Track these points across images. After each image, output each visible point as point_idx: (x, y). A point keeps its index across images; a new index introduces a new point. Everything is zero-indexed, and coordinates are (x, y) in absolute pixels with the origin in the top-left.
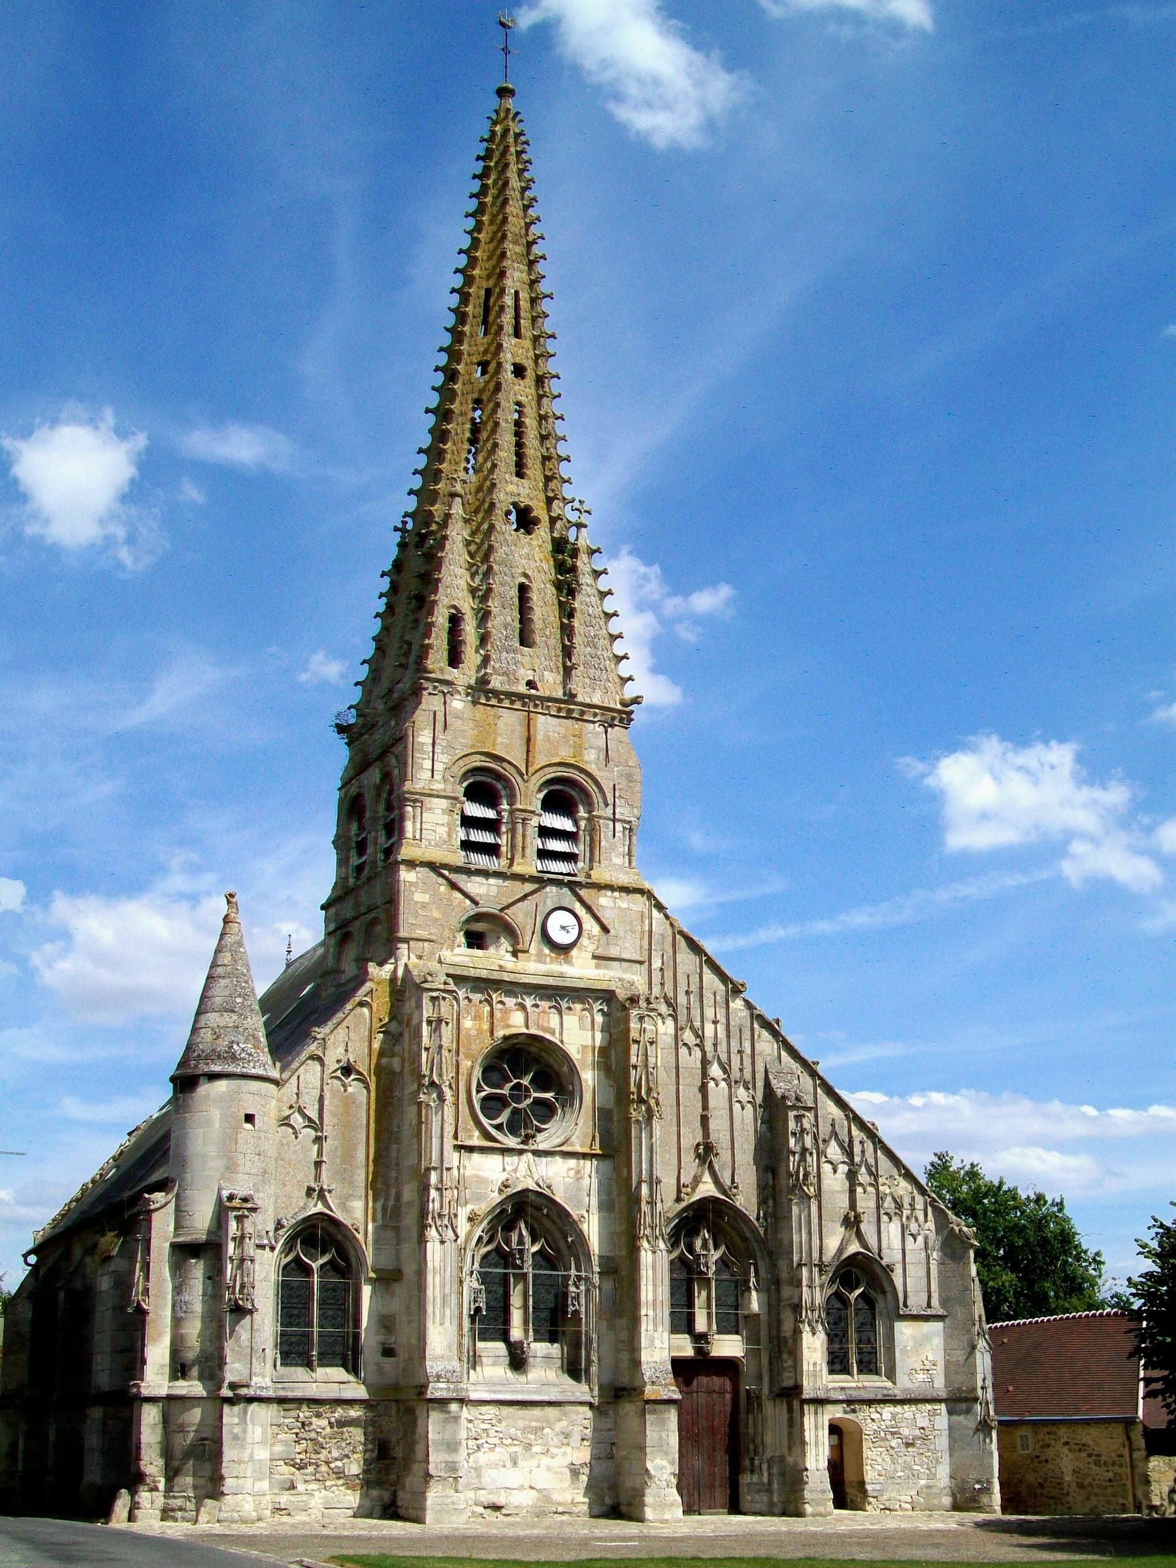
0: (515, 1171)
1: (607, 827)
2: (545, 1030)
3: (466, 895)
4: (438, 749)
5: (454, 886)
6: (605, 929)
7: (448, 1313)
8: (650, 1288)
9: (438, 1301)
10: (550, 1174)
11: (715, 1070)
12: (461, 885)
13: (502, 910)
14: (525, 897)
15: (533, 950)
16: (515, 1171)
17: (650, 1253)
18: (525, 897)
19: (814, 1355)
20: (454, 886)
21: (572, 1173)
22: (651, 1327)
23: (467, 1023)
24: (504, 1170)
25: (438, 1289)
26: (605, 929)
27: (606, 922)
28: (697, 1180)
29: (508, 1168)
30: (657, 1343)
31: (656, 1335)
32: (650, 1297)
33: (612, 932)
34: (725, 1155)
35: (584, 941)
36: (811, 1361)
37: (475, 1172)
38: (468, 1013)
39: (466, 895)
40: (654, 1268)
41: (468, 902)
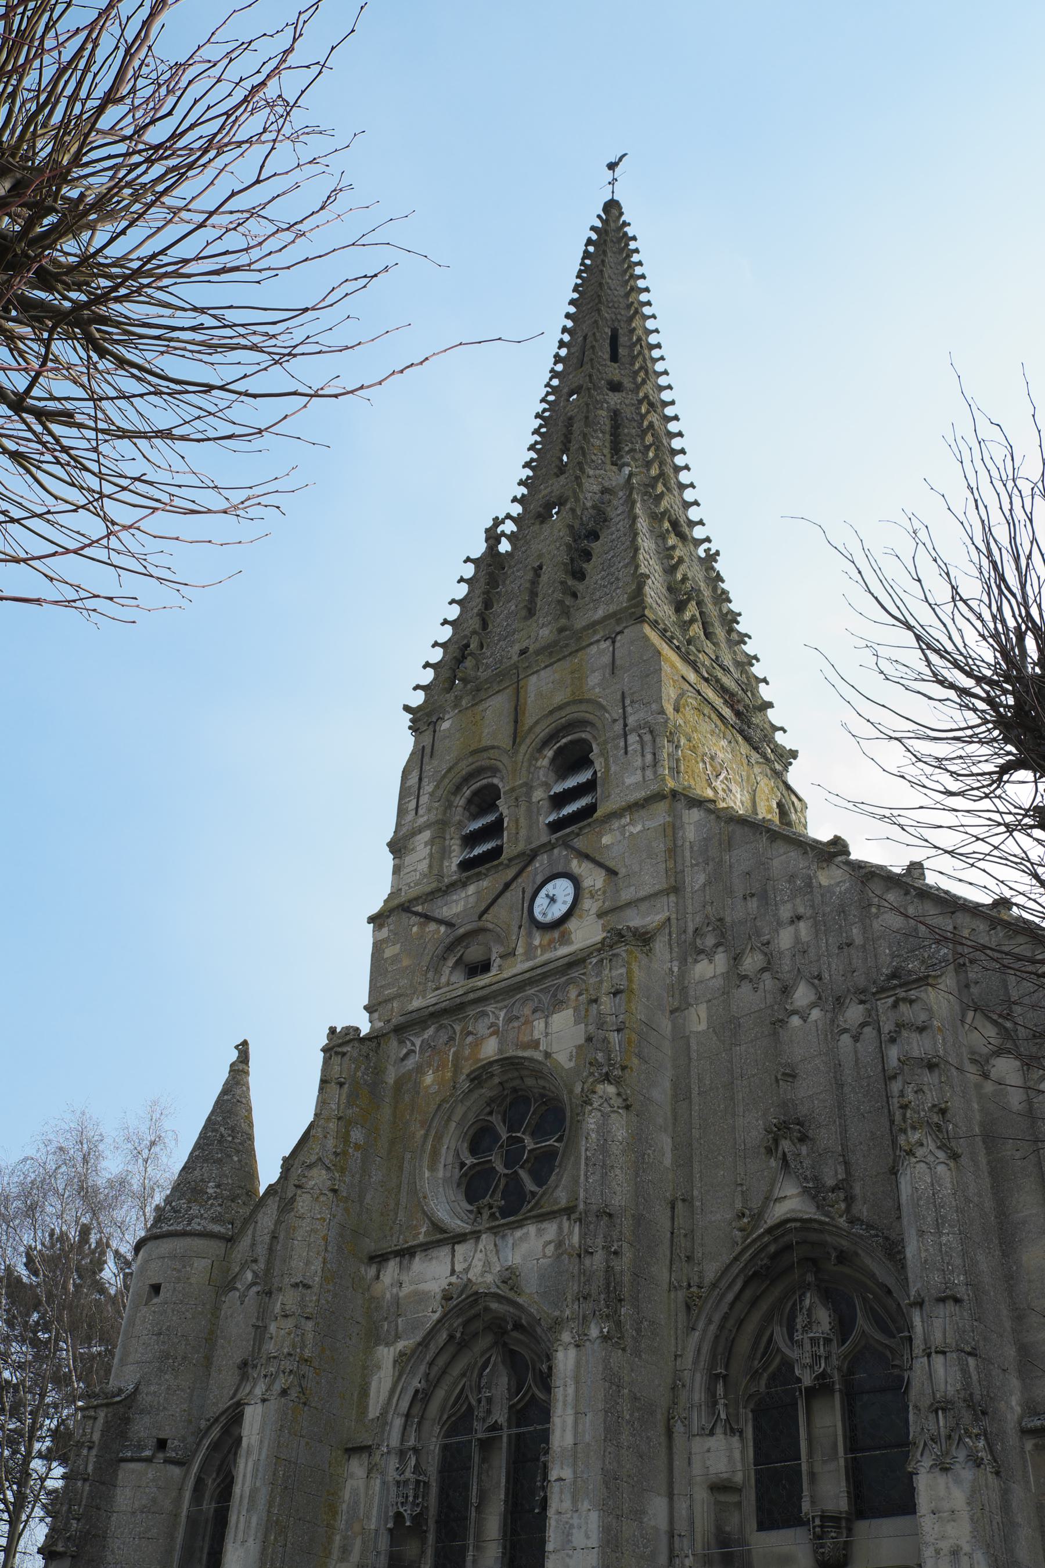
0: (467, 1270)
1: (617, 747)
2: (525, 1046)
3: (440, 922)
4: (425, 781)
5: (428, 918)
6: (612, 872)
7: (254, 1520)
8: (570, 1421)
9: (246, 1501)
10: (518, 1260)
11: (803, 995)
12: (437, 914)
13: (480, 916)
14: (507, 886)
15: (520, 950)
16: (467, 1270)
17: (572, 1352)
18: (507, 886)
19: (950, 1529)
20: (428, 918)
21: (550, 1250)
22: (567, 1504)
23: (429, 1079)
24: (453, 1272)
25: (248, 1483)
26: (612, 872)
27: (611, 864)
28: (769, 1199)
29: (458, 1268)
30: (578, 1538)
31: (575, 1521)
32: (569, 1439)
33: (622, 871)
34: (826, 1137)
35: (587, 904)
36: (945, 1546)
37: (412, 1288)
38: (430, 1065)
39: (440, 922)
40: (577, 1381)
41: (443, 929)
